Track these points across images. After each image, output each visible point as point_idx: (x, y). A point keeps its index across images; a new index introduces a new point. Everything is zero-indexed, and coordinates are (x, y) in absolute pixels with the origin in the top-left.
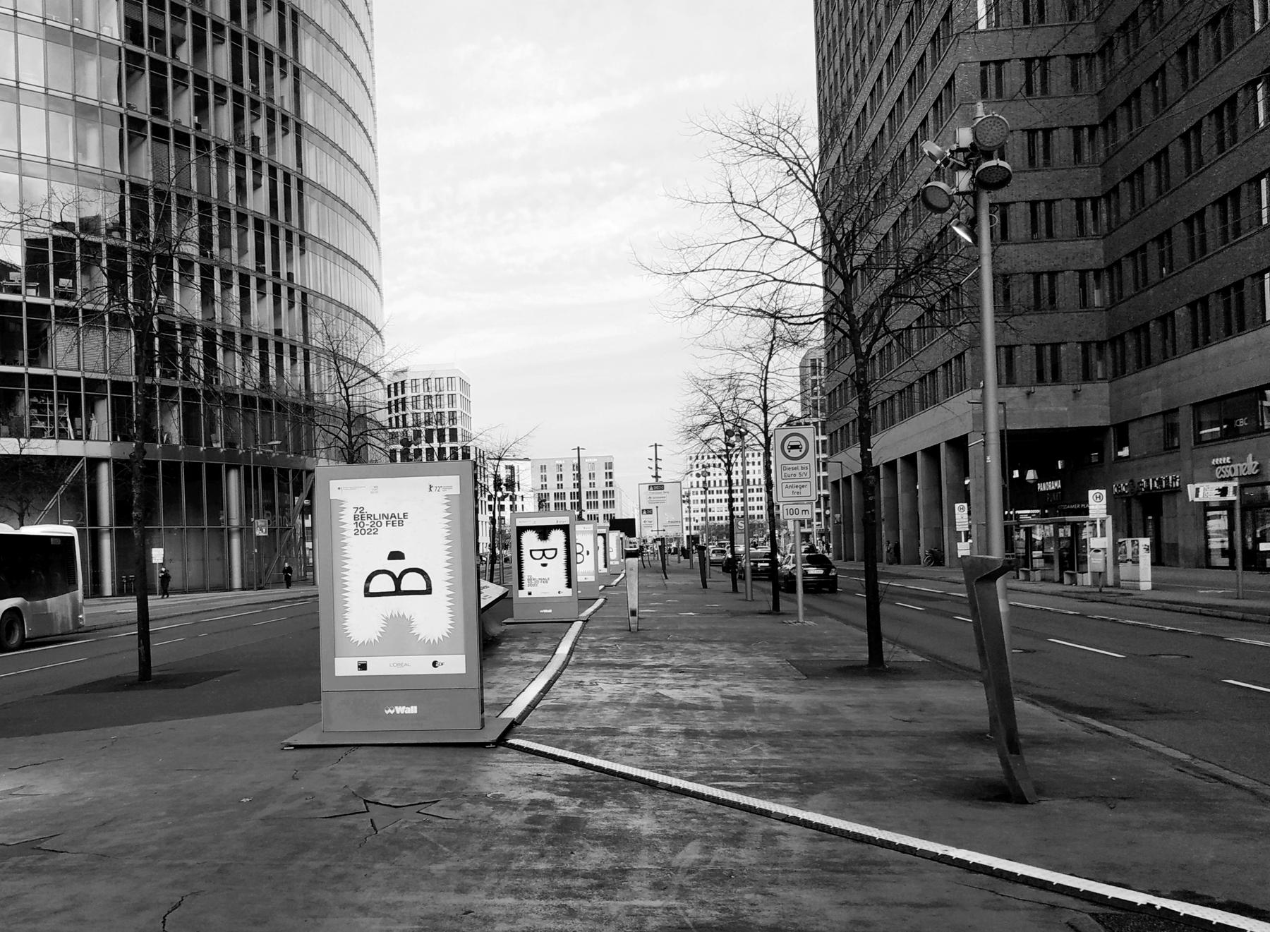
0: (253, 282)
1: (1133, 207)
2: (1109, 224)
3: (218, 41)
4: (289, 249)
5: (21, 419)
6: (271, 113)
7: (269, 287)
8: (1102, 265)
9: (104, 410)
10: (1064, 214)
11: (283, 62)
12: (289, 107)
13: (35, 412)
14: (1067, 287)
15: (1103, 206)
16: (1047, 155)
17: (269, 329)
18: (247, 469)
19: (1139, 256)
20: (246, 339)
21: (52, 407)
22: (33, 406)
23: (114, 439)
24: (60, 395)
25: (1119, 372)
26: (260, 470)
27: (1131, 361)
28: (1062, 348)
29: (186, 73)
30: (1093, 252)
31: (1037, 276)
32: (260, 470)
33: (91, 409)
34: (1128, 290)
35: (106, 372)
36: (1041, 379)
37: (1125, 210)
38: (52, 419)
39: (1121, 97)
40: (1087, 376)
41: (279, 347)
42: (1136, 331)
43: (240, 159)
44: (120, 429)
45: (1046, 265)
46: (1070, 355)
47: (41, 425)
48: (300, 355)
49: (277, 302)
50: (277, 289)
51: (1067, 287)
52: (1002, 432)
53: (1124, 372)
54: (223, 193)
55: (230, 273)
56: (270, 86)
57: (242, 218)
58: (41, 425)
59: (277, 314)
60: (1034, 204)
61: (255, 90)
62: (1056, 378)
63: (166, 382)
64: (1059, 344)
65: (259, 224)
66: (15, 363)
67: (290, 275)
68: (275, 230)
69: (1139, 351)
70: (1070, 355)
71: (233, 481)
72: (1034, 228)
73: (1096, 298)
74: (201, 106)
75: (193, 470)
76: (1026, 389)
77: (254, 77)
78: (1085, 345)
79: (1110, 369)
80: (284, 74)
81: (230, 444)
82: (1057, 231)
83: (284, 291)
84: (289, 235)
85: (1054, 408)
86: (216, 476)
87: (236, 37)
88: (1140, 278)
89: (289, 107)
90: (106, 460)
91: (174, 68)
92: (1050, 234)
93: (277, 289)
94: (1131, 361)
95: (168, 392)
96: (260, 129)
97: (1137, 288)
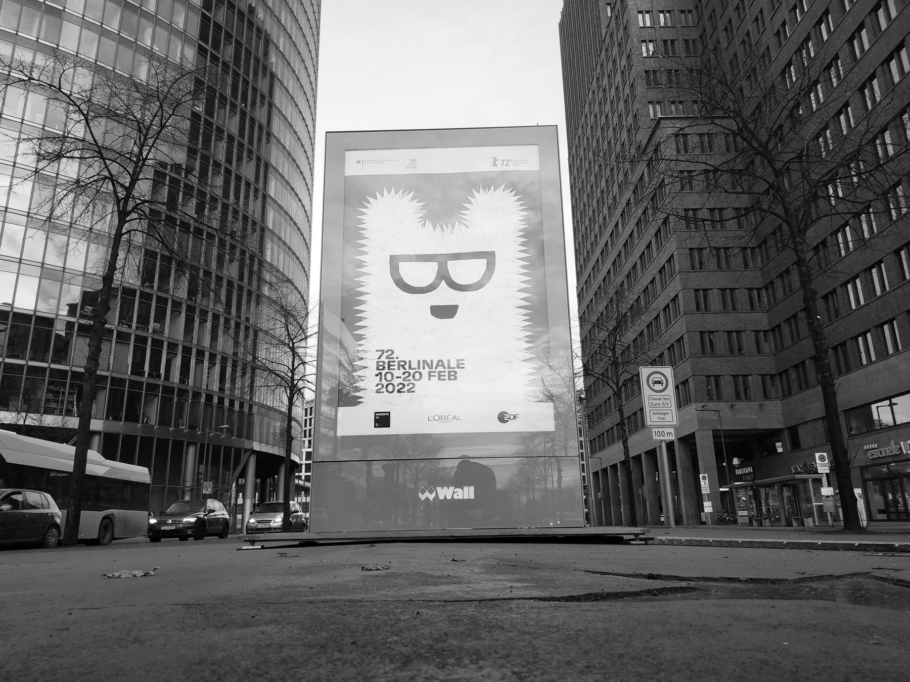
0: (222, 320)
1: (785, 292)
2: (769, 303)
3: (216, 173)
4: (249, 303)
5: (40, 400)
6: (245, 218)
7: (233, 323)
8: (768, 328)
9: (103, 398)
10: (742, 297)
11: (256, 190)
12: (258, 216)
13: (50, 396)
14: (748, 340)
15: (764, 292)
16: (728, 263)
17: (230, 352)
18: (202, 446)
19: (792, 320)
20: (212, 357)
21: (64, 393)
22: (49, 391)
23: (107, 418)
24: (71, 386)
25: (787, 393)
26: (211, 447)
27: (795, 386)
28: (749, 378)
29: (193, 187)
30: (762, 320)
31: (729, 333)
32: (211, 447)
33: (93, 397)
34: (788, 342)
35: (108, 370)
36: (738, 397)
37: (780, 294)
38: (62, 402)
39: (769, 231)
40: (766, 396)
41: (235, 363)
42: (796, 367)
43: (222, 242)
44: (113, 413)
45: (734, 327)
46: (754, 382)
47: (53, 405)
48: (249, 370)
49: (237, 334)
50: (238, 325)
51: (748, 340)
52: (716, 434)
53: (790, 394)
54: (207, 262)
55: (207, 312)
56: (246, 204)
57: (219, 279)
58: (53, 405)
59: (236, 343)
60: (723, 290)
61: (237, 203)
62: (747, 398)
63: (151, 381)
64: (747, 376)
65: (230, 283)
66: (43, 361)
67: (247, 319)
68: (241, 288)
69: (800, 381)
70: (754, 382)
71: (191, 453)
72: (725, 306)
73: (766, 347)
74: (200, 209)
75: (162, 443)
76: (729, 404)
77: (237, 198)
78: (763, 376)
79: (780, 392)
80: (256, 197)
81: (192, 427)
82: (739, 307)
83: (242, 327)
84: (250, 293)
85: (749, 416)
86: (179, 448)
87: (228, 172)
88: (795, 336)
89: (258, 216)
90: (98, 433)
91: (185, 184)
92: (734, 309)
93: (238, 325)
94: (795, 386)
95: (152, 388)
96: (238, 225)
97: (793, 341)
